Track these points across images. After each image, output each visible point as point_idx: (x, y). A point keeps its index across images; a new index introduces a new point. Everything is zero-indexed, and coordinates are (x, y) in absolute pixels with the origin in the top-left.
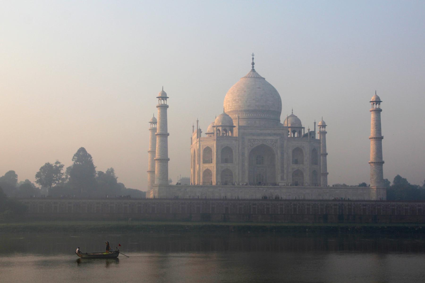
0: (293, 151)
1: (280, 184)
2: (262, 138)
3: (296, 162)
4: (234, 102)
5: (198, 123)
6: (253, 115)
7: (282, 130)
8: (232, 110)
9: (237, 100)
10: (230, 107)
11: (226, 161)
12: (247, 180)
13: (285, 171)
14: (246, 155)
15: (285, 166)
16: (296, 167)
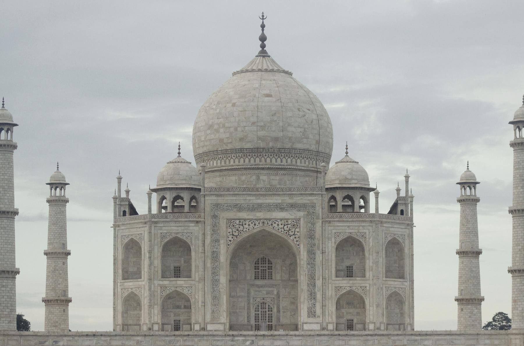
0: (340, 247)
1: (306, 327)
2: (260, 215)
3: (349, 273)
4: (209, 132)
5: (119, 183)
6: (252, 160)
7: (311, 195)
8: (205, 149)
9: (216, 127)
10: (202, 144)
11: (177, 273)
12: (224, 318)
13: (319, 296)
14: (224, 257)
15: (319, 283)
16: (345, 284)
